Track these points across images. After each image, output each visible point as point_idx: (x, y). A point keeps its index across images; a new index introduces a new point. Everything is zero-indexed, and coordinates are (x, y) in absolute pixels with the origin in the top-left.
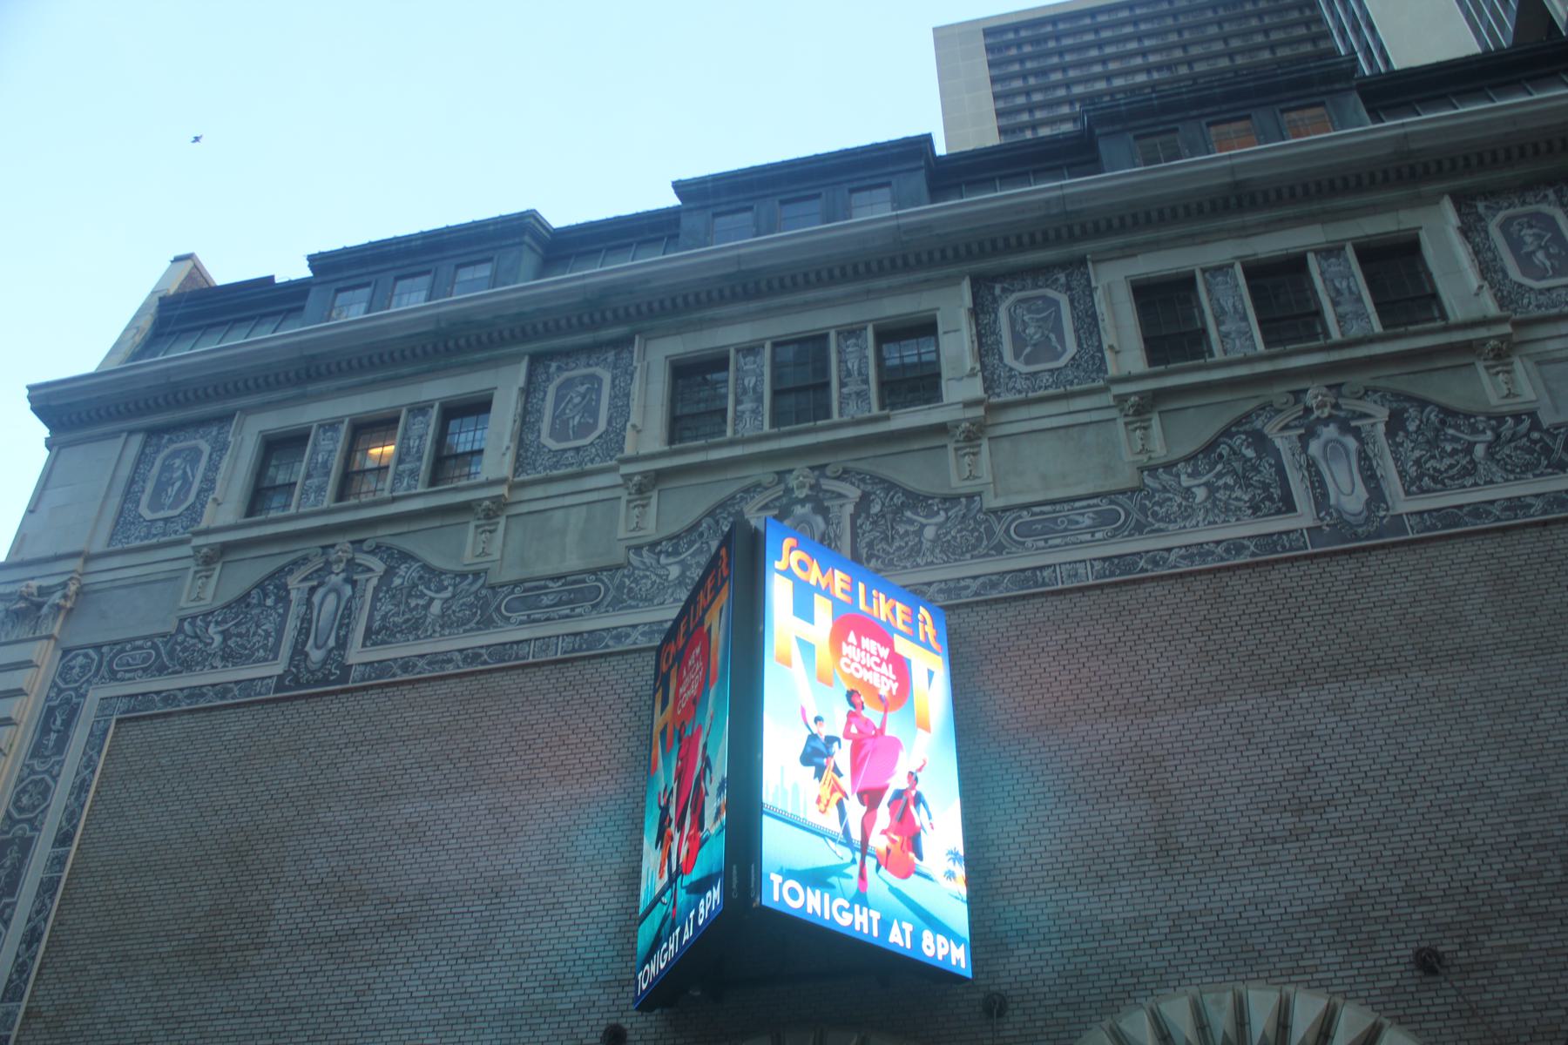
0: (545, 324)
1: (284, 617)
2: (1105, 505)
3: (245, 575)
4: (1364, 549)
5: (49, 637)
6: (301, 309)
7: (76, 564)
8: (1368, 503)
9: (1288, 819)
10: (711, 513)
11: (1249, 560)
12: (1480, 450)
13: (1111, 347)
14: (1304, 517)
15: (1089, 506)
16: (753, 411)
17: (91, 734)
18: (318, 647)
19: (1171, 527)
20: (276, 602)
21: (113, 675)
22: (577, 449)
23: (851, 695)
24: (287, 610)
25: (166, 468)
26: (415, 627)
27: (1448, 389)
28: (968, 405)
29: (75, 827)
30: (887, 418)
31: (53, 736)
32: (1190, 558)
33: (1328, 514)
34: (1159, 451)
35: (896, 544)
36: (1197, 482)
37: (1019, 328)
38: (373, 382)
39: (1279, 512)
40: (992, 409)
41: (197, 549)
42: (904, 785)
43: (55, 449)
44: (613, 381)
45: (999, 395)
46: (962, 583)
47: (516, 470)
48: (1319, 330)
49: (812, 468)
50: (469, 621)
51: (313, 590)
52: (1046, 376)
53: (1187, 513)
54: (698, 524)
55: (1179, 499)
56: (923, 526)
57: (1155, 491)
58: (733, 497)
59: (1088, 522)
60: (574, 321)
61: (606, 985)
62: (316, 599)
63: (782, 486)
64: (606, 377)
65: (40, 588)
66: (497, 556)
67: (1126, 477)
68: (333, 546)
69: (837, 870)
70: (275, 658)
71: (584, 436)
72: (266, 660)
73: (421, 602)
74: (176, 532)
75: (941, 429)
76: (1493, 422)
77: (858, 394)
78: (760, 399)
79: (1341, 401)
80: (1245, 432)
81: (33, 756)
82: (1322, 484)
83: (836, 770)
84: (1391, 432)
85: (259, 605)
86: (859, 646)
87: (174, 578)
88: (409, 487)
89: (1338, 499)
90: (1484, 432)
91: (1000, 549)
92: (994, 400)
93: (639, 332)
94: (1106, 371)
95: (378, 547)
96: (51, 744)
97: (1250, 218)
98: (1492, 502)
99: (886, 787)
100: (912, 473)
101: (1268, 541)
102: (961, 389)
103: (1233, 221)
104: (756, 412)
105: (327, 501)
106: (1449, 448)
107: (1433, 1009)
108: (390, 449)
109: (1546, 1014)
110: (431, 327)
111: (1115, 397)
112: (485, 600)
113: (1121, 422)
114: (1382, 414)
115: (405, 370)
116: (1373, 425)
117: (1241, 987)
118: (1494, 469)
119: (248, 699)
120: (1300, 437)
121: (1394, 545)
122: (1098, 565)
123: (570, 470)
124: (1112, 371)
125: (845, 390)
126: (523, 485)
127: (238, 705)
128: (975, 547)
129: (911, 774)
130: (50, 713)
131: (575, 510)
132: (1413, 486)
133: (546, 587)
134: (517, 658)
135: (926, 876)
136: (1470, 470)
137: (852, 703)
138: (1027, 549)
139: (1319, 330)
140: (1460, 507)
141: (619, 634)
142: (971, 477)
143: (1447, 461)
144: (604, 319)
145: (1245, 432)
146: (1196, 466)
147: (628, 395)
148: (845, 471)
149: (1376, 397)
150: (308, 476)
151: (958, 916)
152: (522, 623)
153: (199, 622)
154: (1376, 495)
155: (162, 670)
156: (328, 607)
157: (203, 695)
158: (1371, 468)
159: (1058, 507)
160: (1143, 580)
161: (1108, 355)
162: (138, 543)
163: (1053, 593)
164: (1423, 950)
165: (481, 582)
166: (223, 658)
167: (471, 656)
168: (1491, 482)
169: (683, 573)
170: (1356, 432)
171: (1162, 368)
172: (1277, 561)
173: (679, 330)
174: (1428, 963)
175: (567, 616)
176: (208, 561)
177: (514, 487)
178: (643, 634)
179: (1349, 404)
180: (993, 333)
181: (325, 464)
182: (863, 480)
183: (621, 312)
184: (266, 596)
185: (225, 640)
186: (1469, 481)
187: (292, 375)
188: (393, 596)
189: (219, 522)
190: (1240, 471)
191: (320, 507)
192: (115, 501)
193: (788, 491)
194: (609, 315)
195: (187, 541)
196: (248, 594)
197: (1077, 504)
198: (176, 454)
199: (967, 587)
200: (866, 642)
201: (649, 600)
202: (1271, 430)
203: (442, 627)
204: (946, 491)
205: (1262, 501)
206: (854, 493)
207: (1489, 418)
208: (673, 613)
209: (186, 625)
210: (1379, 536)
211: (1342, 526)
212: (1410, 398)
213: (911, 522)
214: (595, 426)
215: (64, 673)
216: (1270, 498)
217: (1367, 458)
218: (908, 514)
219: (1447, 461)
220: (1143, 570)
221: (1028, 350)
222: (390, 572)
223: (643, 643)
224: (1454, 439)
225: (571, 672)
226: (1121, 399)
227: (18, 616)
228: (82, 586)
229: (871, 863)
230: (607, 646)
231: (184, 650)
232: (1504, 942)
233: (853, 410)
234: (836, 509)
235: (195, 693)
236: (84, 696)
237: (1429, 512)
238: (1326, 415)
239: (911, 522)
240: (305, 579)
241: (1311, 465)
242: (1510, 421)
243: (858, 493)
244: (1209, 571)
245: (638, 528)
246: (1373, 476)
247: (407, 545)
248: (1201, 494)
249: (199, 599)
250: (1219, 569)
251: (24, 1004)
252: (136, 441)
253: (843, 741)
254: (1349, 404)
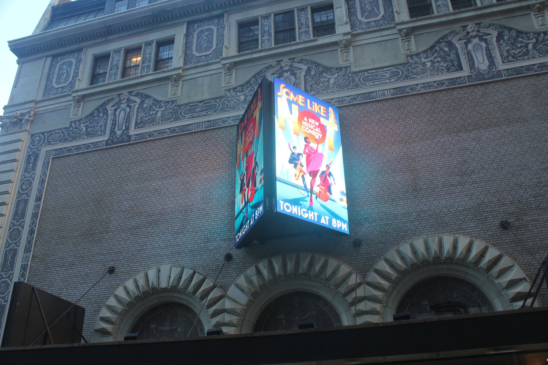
0: (192, 10)
1: (106, 120)
2: (394, 70)
3: (92, 106)
4: (487, 83)
5: (26, 131)
6: (104, 9)
7: (33, 105)
8: (489, 67)
9: (458, 178)
10: (254, 77)
11: (446, 88)
12: (530, 46)
13: (397, 12)
14: (466, 72)
15: (389, 70)
16: (268, 39)
17: (44, 163)
18: (119, 130)
19: (418, 77)
20: (103, 115)
21: (49, 143)
22: (206, 55)
23: (306, 139)
24: (107, 117)
25: (61, 69)
26: (152, 121)
27: (520, 24)
28: (345, 34)
29: (42, 195)
30: (316, 40)
31: (31, 165)
32: (425, 87)
33: (475, 71)
34: (414, 49)
35: (320, 85)
36: (428, 60)
37: (363, 5)
38: (132, 34)
39: (457, 70)
40: (354, 36)
41: (74, 97)
42: (325, 169)
43: (20, 64)
44: (217, 30)
45: (356, 31)
46: (344, 99)
47: (184, 64)
48: (473, 3)
49: (290, 59)
50: (171, 118)
51: (116, 110)
52: (373, 23)
53: (424, 71)
54: (250, 80)
55: (421, 67)
56: (330, 79)
57: (412, 64)
58: (262, 71)
59: (388, 76)
60: (202, 9)
61: (225, 240)
62: (117, 113)
63: (279, 66)
64: (215, 29)
65: (21, 114)
66: (179, 95)
67: (402, 59)
68: (122, 94)
69: (303, 199)
70: (105, 134)
71: (208, 51)
72: (101, 135)
73: (154, 112)
74: (66, 92)
75: (335, 43)
76: (536, 35)
77: (305, 32)
78: (270, 35)
79: (480, 29)
80: (445, 42)
81: (25, 172)
82: (473, 60)
83: (301, 165)
84: (498, 40)
85: (98, 116)
86: (308, 121)
87: (67, 108)
88: (147, 72)
89: (478, 65)
90: (532, 39)
91: (357, 86)
92: (354, 32)
93: (226, 12)
94: (395, 21)
95: (137, 94)
96: (31, 167)
98: (534, 65)
99: (319, 170)
100: (325, 60)
101: (452, 81)
102: (342, 28)
104: (269, 40)
105: (119, 78)
106: (519, 45)
107: (506, 241)
108: (139, 59)
109: (544, 242)
110: (151, 13)
111: (398, 30)
112: (176, 110)
113: (400, 39)
114: (495, 34)
116: (492, 38)
117: (441, 235)
118: (535, 53)
119: (96, 149)
120: (465, 43)
121: (498, 81)
122: (392, 91)
123: (203, 63)
124: (397, 20)
125: (301, 31)
126: (188, 69)
127: (93, 151)
128: (348, 86)
129: (327, 165)
130: (29, 157)
131: (206, 77)
132: (505, 60)
133: (198, 105)
134: (189, 130)
135: (333, 200)
136: (527, 53)
137: (306, 142)
138: (367, 86)
139: (473, 3)
140: (522, 67)
141: (224, 121)
142: (346, 60)
143: (518, 50)
144: (213, 8)
145: (445, 42)
146: (427, 54)
147: (223, 35)
148: (302, 60)
149: (493, 27)
150: (111, 70)
151: (344, 214)
152: (190, 118)
153: (77, 123)
154: (492, 63)
155: (66, 140)
157: (81, 148)
158: (490, 53)
159: (378, 71)
160: (408, 96)
161: (396, 15)
162: (53, 96)
163: (376, 101)
164: (503, 221)
165: (174, 104)
166: (86, 135)
167: (173, 130)
168: (534, 57)
169: (245, 99)
170: (485, 41)
171: (415, 19)
172: (456, 88)
173: (240, 11)
174: (505, 226)
175: (205, 115)
176: (78, 101)
177: (184, 70)
178: (232, 120)
179: (483, 30)
180: (354, 8)
181: (117, 65)
182: (308, 63)
183: (219, 5)
184: (100, 113)
185: (87, 129)
186: (526, 57)
187: (102, 33)
188: (144, 111)
189: (81, 88)
190: (443, 56)
191: (116, 80)
192: (44, 82)
193: (281, 68)
194: (215, 6)
195: (71, 95)
196: (93, 112)
197: (385, 69)
198: (63, 64)
199: (346, 100)
200: (310, 120)
201: (234, 108)
202: (455, 41)
203: (162, 121)
204: (338, 66)
205: (451, 67)
206: (305, 68)
207: (535, 34)
208: (242, 113)
209: (73, 124)
210: (493, 78)
211: (479, 75)
212: (505, 27)
213: (325, 77)
214: (212, 47)
215: (33, 142)
216: (454, 65)
217: (489, 50)
218: (324, 74)
219: (518, 50)
220: (408, 92)
221: (366, 13)
222: (142, 102)
223: (232, 123)
224: (522, 42)
225: (208, 134)
226: (400, 31)
227: (14, 124)
228: (35, 113)
229: (314, 196)
230: (220, 125)
231: (73, 133)
232: (531, 218)
233: (304, 38)
234: (299, 73)
235: (78, 147)
236: (40, 150)
237: (511, 69)
238: (474, 34)
239: (325, 77)
240: (112, 107)
241: (469, 53)
242: (542, 35)
243: (306, 67)
244: (431, 92)
245: (229, 83)
246: (491, 57)
247: (147, 92)
248: (429, 64)
249: (76, 115)
250: (435, 91)
251: (31, 253)
252: (49, 60)
253: (303, 155)
254: (483, 30)
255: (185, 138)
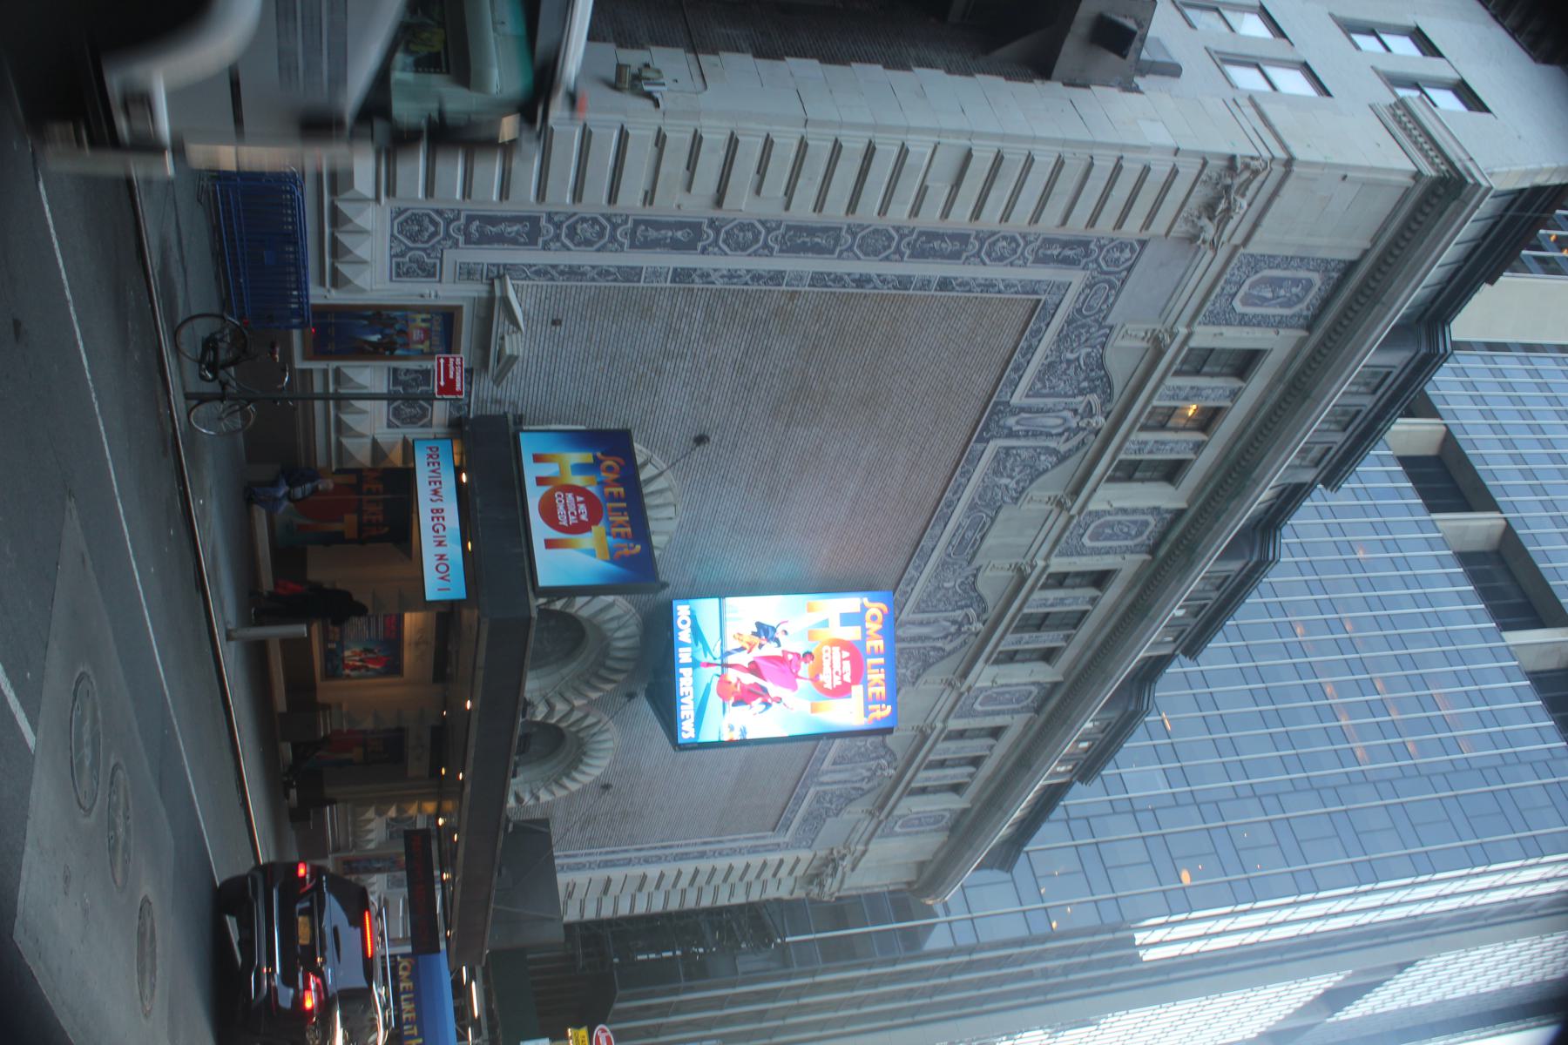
38: (1249, 424)
97: (1009, 764)
103: (1013, 758)
115: (1239, 446)
154: (822, 784)
156: (1051, 421)
174: (606, 787)
226: (933, 729)
255: (921, 522)
